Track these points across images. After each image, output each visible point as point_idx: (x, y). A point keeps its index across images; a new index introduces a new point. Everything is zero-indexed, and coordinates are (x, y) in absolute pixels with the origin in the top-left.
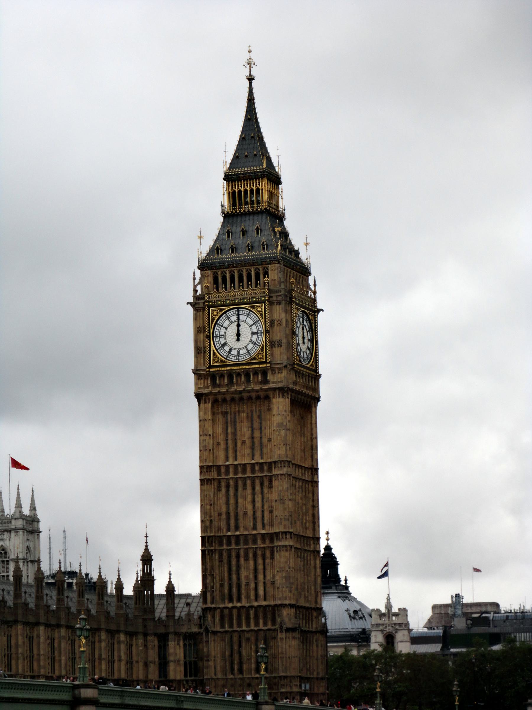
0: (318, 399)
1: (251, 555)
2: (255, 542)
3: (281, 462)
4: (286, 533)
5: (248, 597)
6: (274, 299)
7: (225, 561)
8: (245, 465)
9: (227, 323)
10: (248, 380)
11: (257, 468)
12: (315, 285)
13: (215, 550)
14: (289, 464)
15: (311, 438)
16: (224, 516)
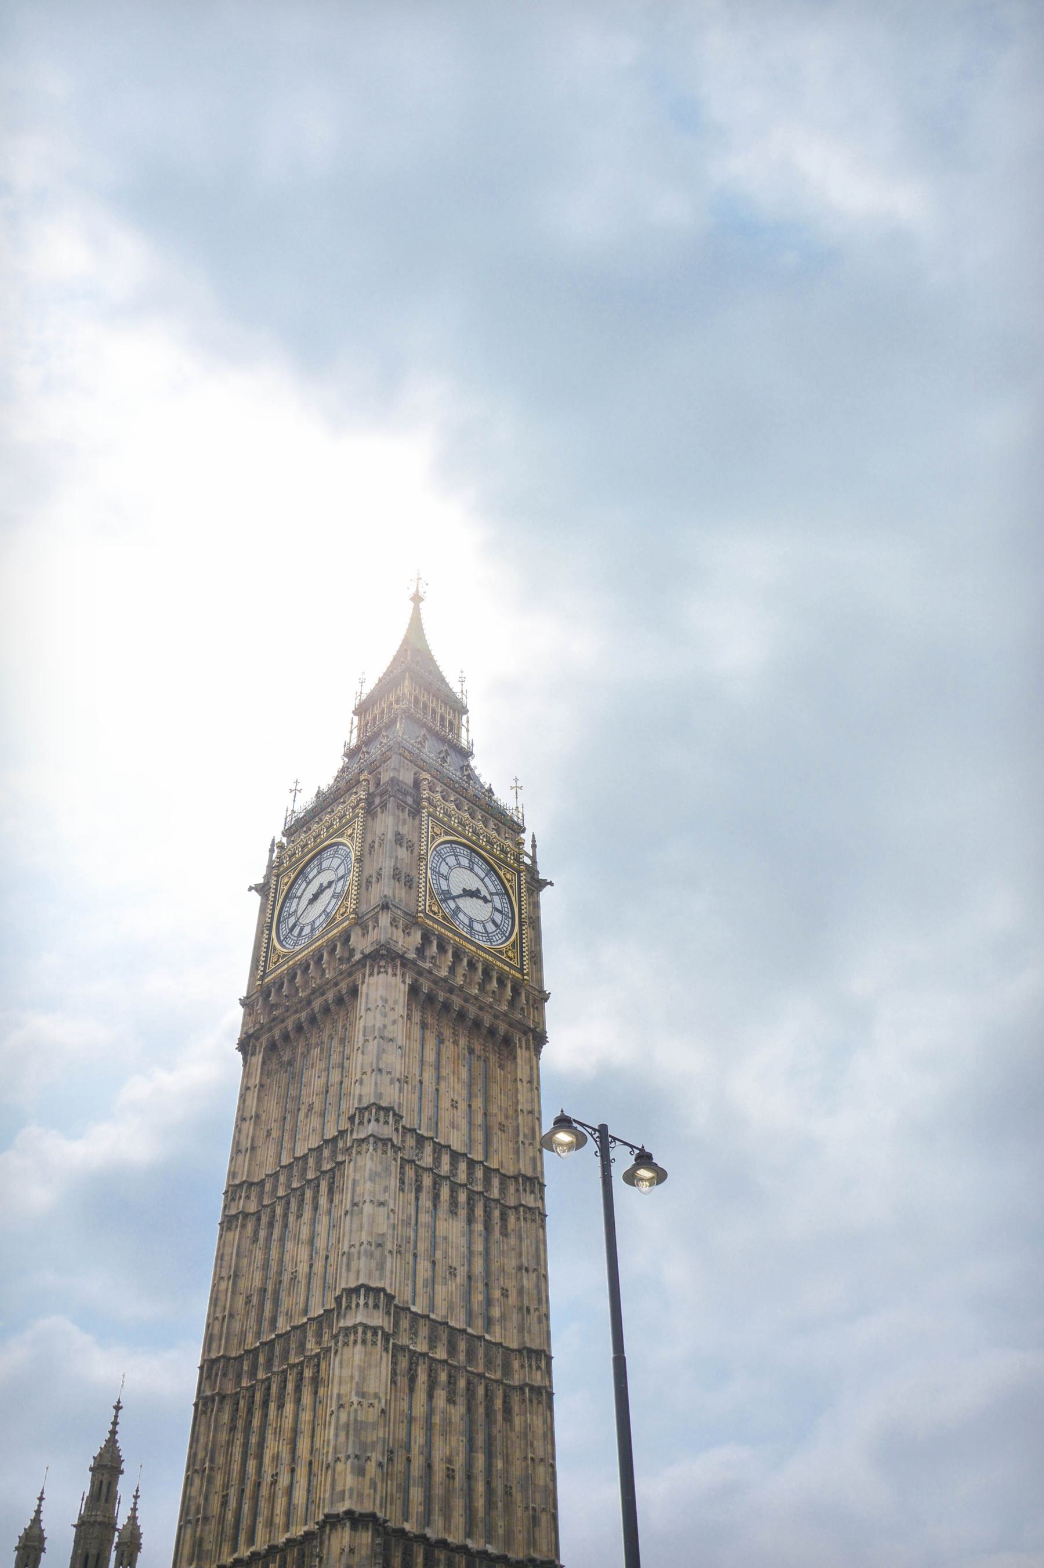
0: (540, 1039)
1: (290, 1386)
2: (302, 1346)
3: (361, 1110)
4: (356, 1290)
5: (270, 1523)
6: (377, 801)
7: (240, 1424)
8: (305, 1157)
9: (304, 884)
10: (324, 971)
11: (326, 1153)
12: (534, 846)
13: (223, 1398)
14: (387, 1115)
15: (516, 1111)
16: (255, 1300)
